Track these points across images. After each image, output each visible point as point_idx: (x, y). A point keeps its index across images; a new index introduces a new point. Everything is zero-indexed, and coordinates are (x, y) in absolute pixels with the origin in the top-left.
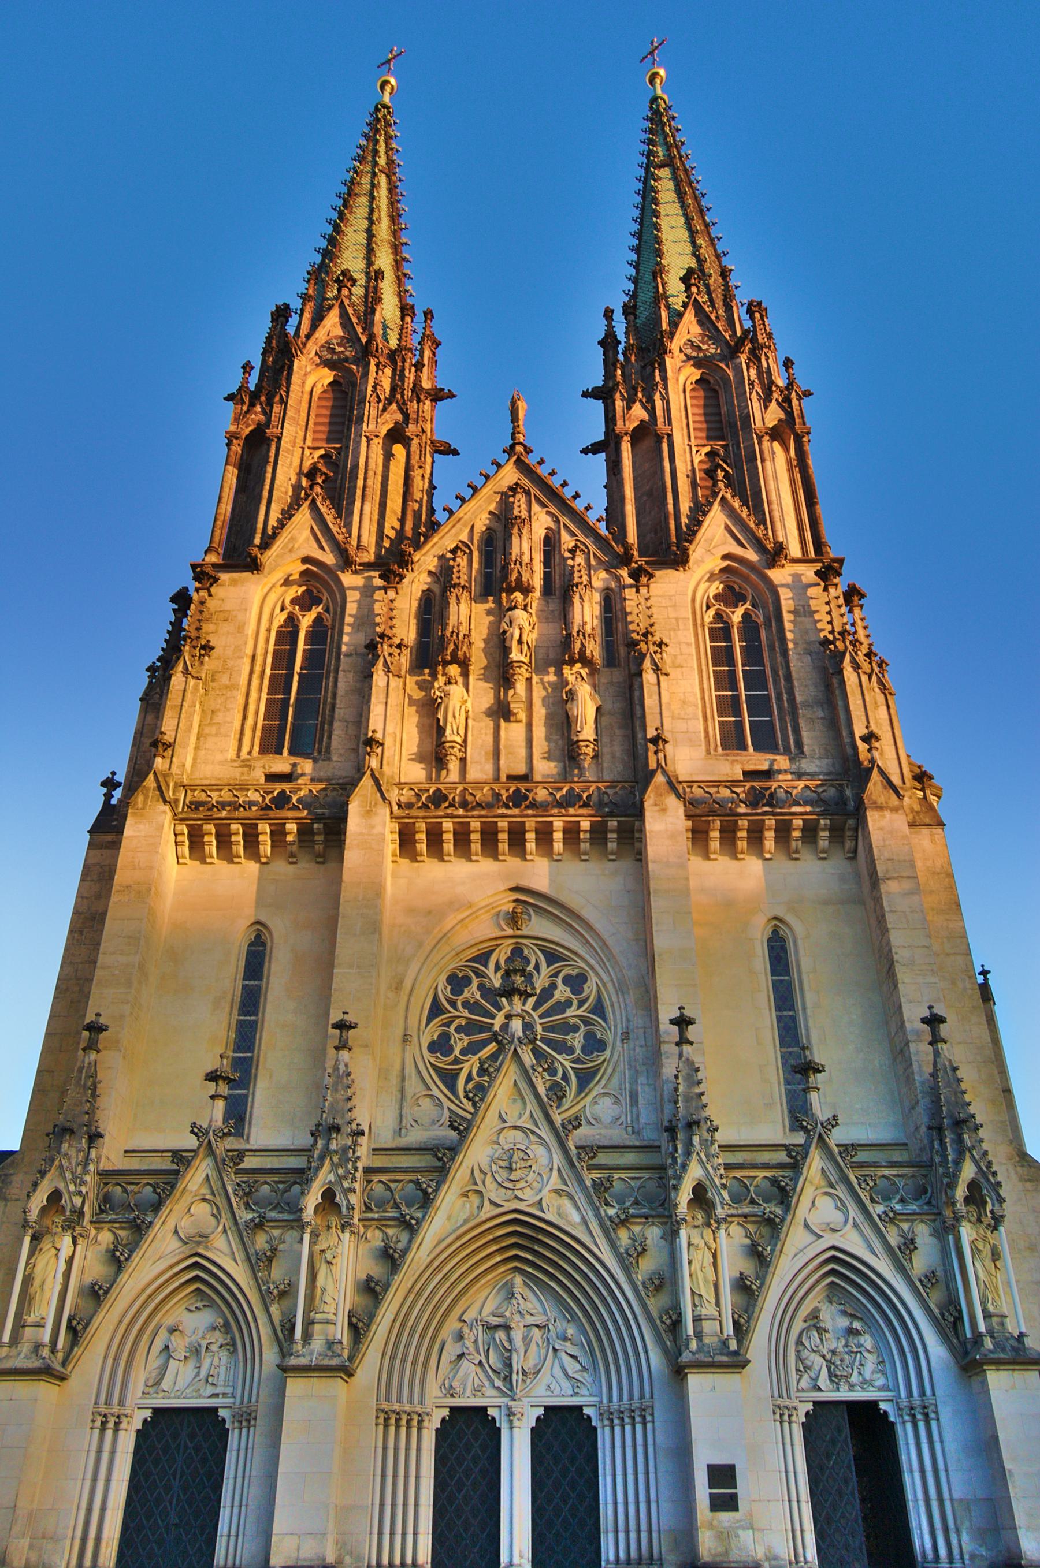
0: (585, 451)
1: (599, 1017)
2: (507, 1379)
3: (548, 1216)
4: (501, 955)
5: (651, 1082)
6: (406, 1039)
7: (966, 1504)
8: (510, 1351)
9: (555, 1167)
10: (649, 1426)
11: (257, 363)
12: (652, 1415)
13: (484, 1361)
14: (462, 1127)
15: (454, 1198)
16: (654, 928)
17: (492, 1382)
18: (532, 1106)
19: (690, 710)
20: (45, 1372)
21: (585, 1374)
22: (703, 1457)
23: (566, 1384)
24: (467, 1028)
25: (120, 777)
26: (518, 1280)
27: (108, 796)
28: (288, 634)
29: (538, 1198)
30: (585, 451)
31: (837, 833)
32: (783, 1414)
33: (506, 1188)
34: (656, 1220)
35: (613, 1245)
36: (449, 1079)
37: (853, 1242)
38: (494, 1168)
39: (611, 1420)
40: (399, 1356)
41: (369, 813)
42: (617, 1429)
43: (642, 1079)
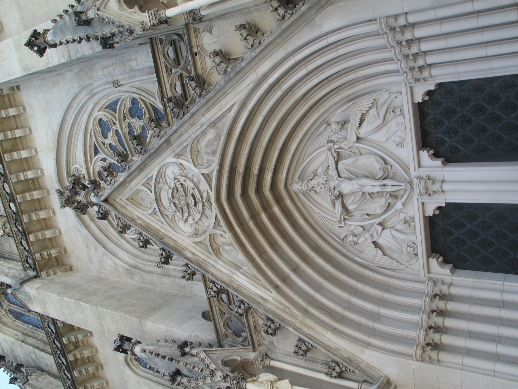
1: (117, 105)
2: (394, 196)
3: (215, 166)
5: (134, 57)
8: (363, 193)
9: (174, 160)
10: (412, 19)
12: (396, 17)
13: (378, 220)
15: (220, 262)
16: (13, 78)
17: (400, 211)
18: (137, 184)
21: (381, 101)
23: (394, 124)
26: (295, 187)
29: (202, 178)
33: (203, 209)
34: (194, 43)
35: (222, 91)
38: (190, 219)
39: (421, 68)
40: (370, 323)
42: (430, 60)
43: (134, 65)
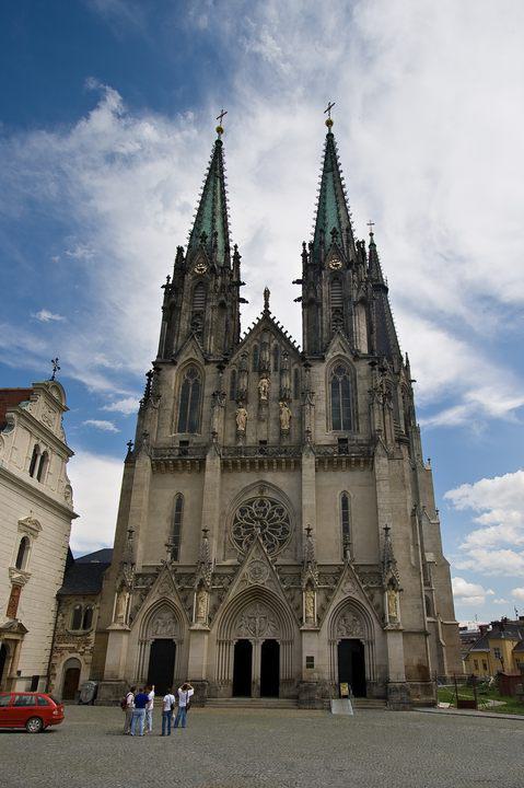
0: (295, 301)
4: (256, 503)
6: (226, 531)
7: (380, 666)
11: (172, 276)
14: (242, 563)
19: (322, 417)
20: (125, 631)
22: (306, 654)
24: (245, 526)
25: (133, 442)
27: (130, 449)
28: (185, 387)
30: (295, 301)
31: (366, 462)
32: (331, 643)
36: (240, 543)
37: (356, 596)
41: (212, 458)
